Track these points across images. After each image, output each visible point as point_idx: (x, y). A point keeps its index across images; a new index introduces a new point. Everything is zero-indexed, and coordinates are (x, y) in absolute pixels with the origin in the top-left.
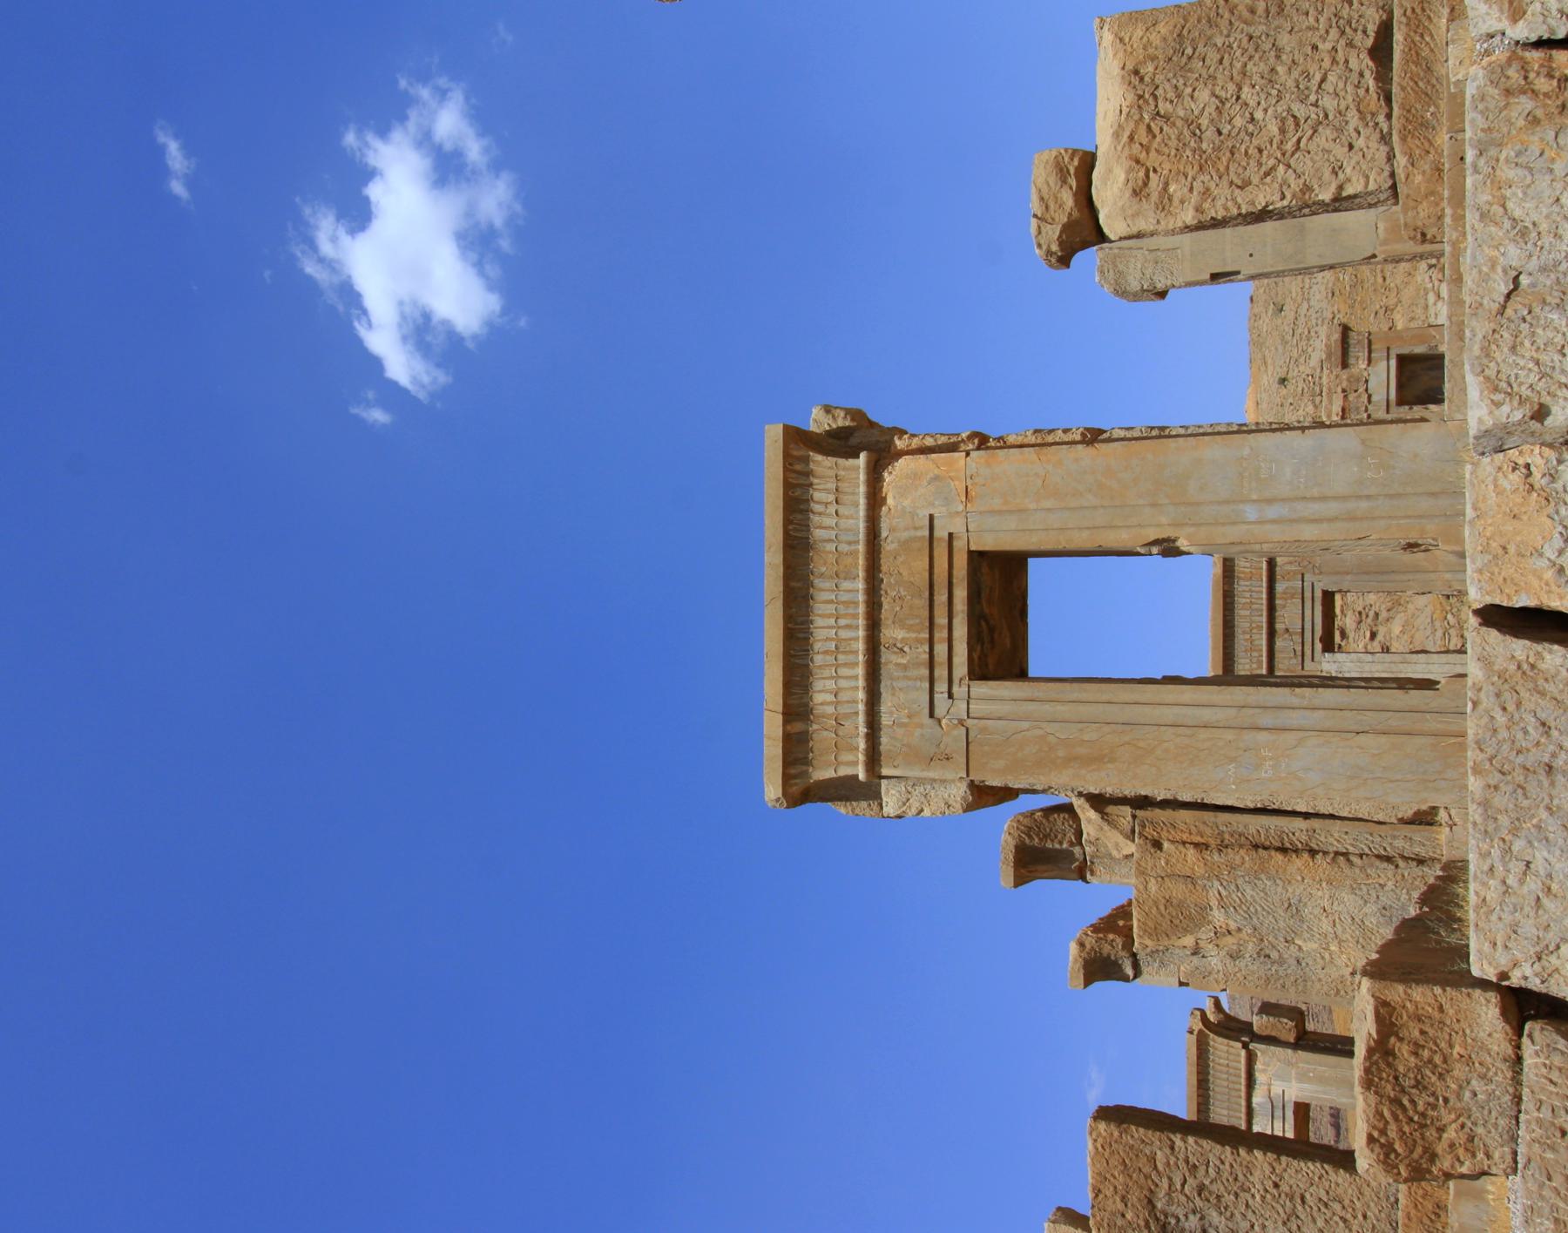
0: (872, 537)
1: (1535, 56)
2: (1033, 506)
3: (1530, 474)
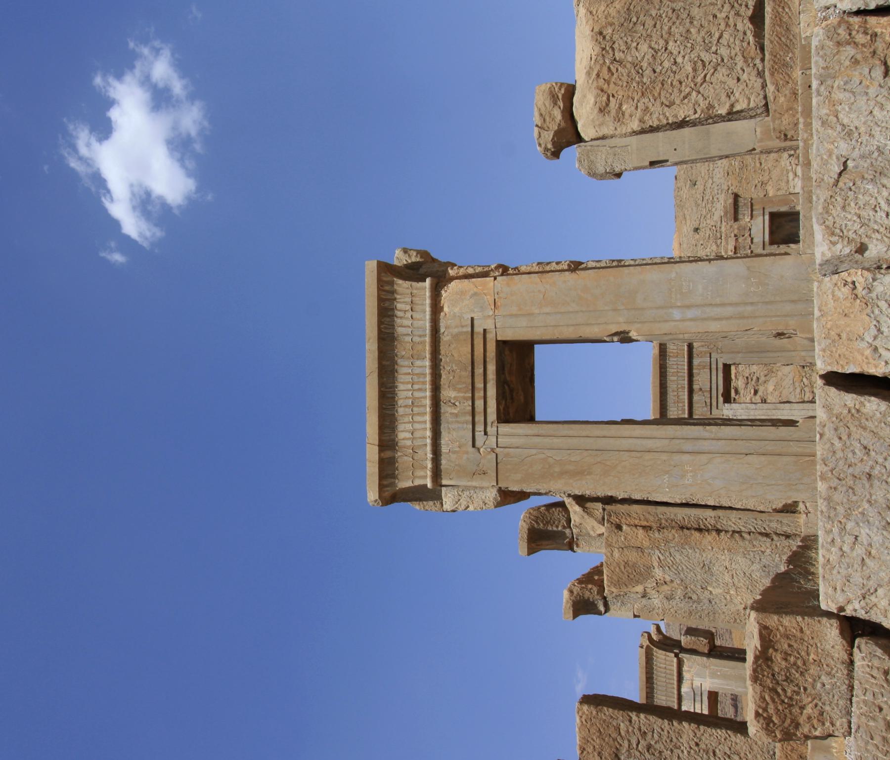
0: (434, 333)
1: (856, 20)
2: (537, 311)
3: (855, 288)
